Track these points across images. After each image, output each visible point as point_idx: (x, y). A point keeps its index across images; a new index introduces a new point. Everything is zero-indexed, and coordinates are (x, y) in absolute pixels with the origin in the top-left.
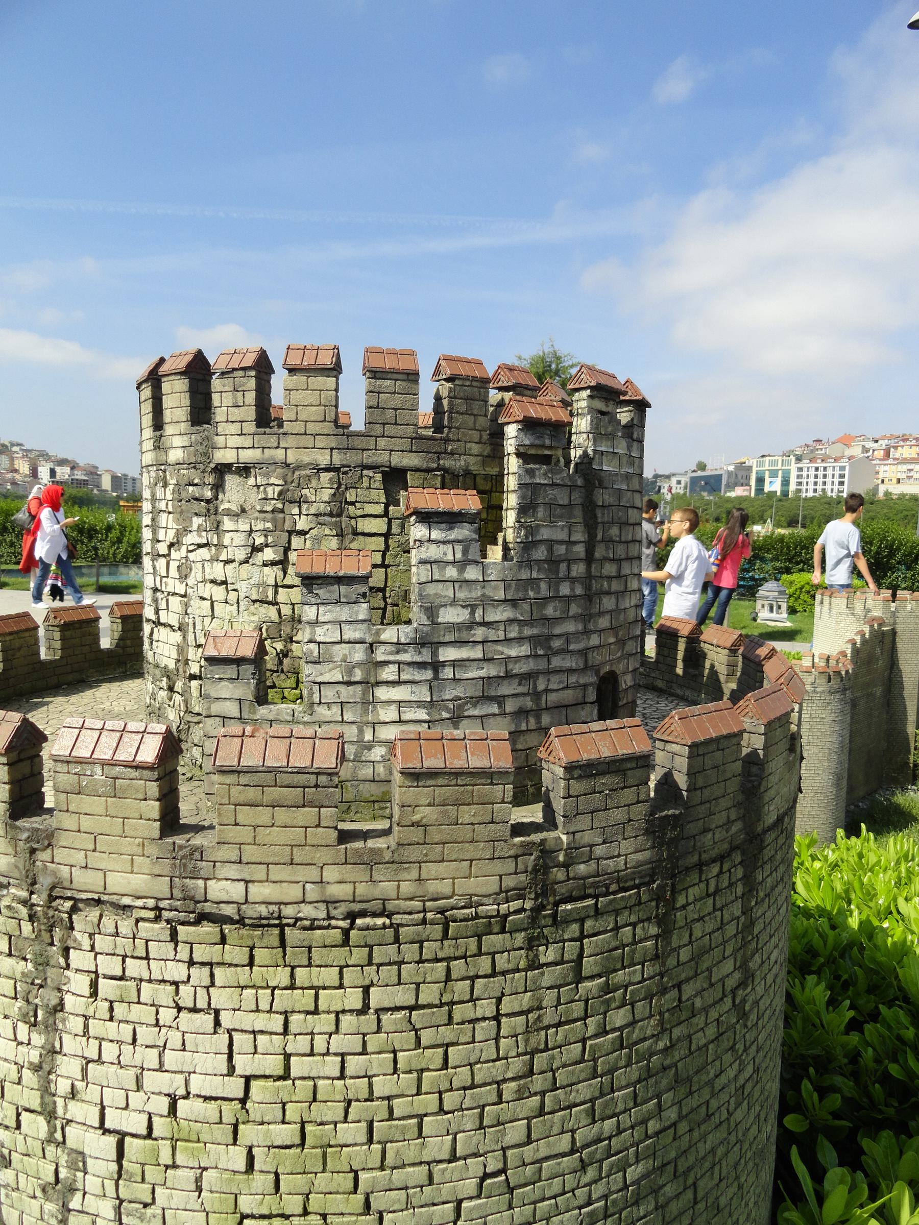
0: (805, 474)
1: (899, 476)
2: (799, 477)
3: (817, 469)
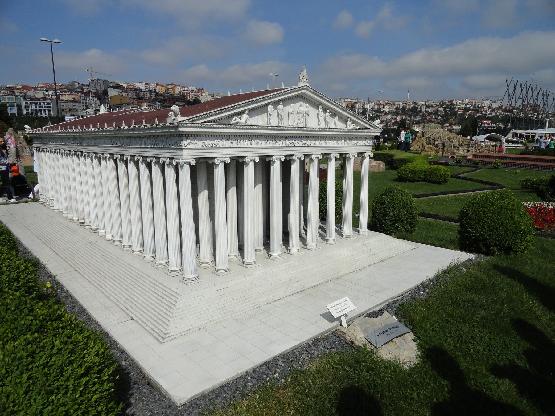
0: (29, 105)
1: (70, 107)
2: (26, 107)
3: (35, 103)
